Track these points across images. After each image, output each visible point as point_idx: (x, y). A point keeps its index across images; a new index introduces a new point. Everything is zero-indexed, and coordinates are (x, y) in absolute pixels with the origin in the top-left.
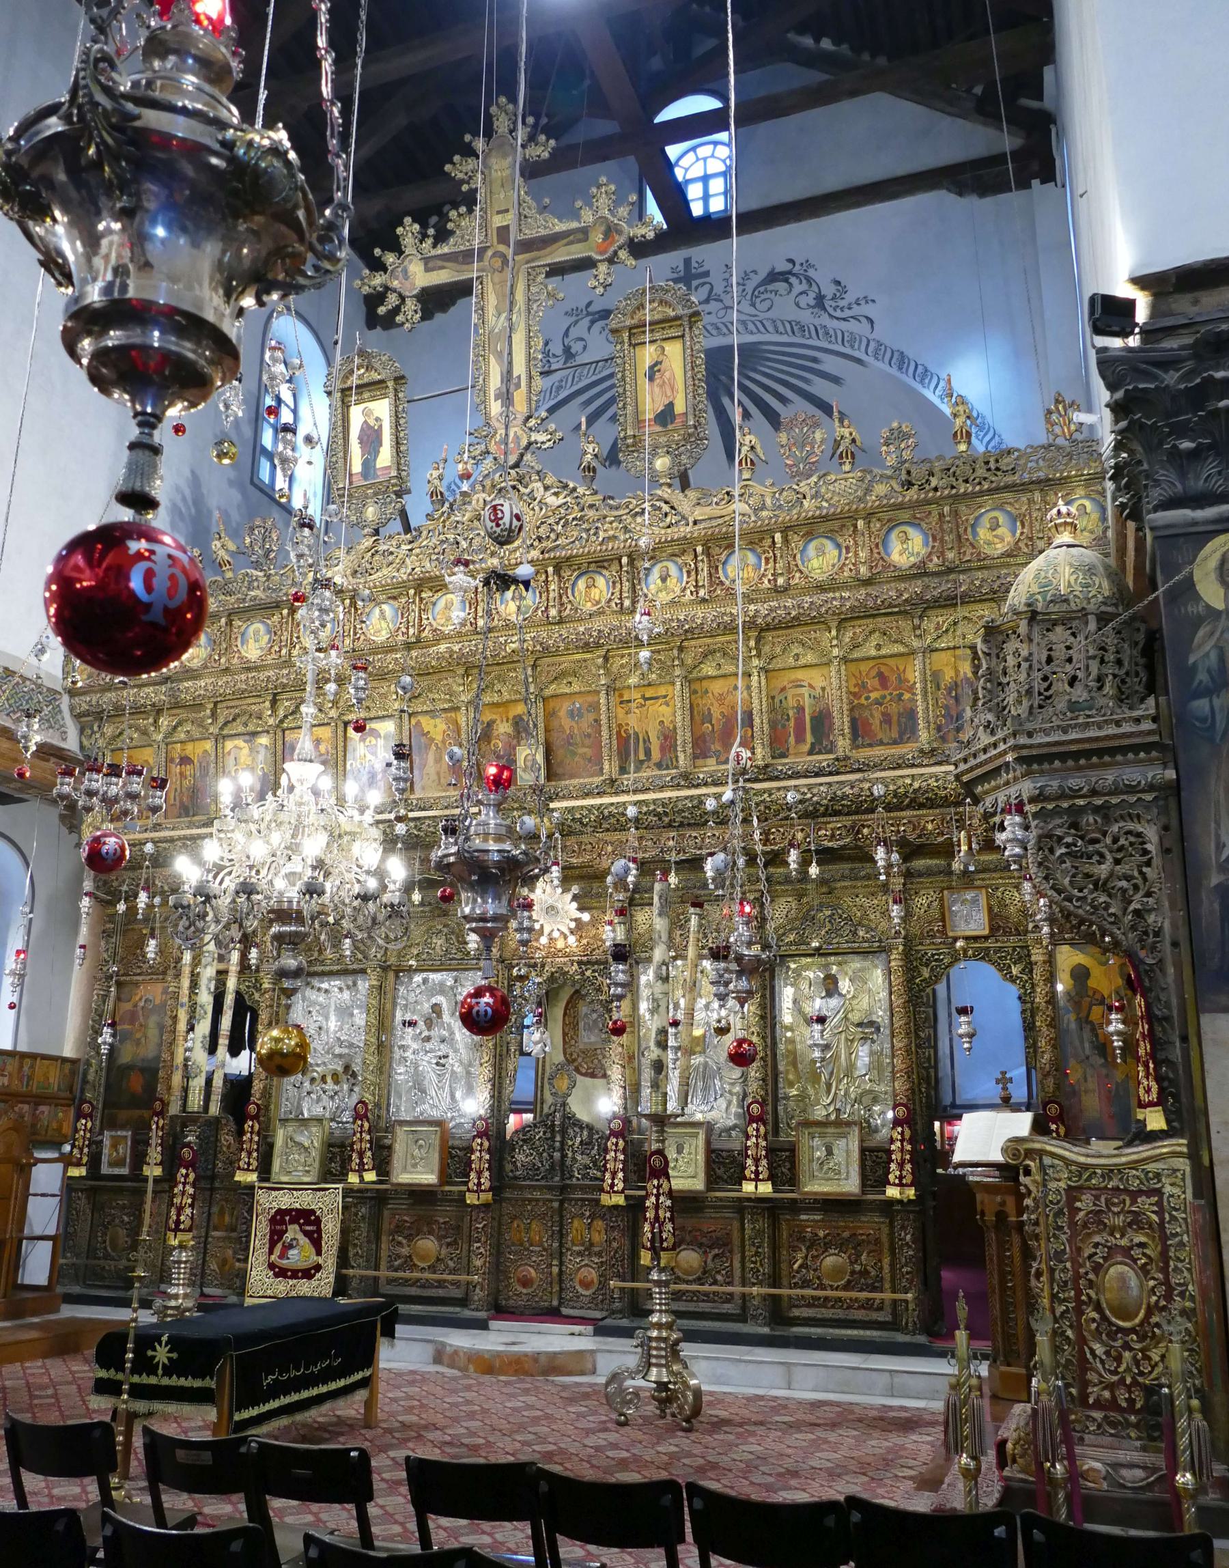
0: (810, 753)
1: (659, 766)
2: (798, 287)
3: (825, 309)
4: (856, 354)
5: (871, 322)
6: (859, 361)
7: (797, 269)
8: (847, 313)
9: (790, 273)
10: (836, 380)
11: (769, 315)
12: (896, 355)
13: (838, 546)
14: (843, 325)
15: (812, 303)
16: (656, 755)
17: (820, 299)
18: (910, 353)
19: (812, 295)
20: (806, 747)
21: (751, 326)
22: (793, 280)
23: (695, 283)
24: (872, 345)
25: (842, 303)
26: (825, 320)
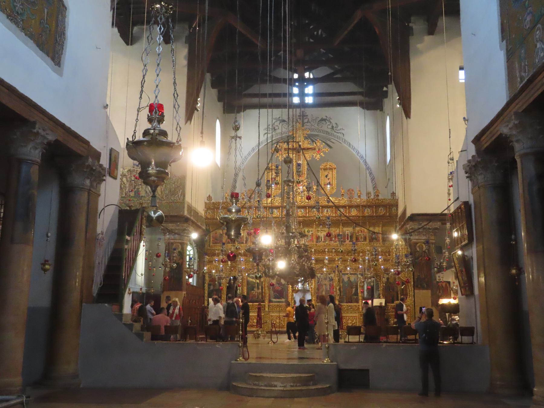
0: (350, 242)
1: (323, 242)
2: (328, 123)
3: (333, 129)
4: (340, 141)
5: (343, 134)
6: (340, 143)
7: (328, 119)
8: (338, 131)
9: (326, 119)
10: (333, 143)
11: (322, 128)
12: (348, 143)
13: (357, 210)
14: (338, 134)
15: (331, 127)
16: (323, 240)
17: (333, 127)
18: (351, 143)
19: (331, 126)
20: (349, 241)
21: (317, 131)
22: (327, 121)
23: (305, 117)
24: (343, 140)
25: (337, 129)
26: (333, 132)
